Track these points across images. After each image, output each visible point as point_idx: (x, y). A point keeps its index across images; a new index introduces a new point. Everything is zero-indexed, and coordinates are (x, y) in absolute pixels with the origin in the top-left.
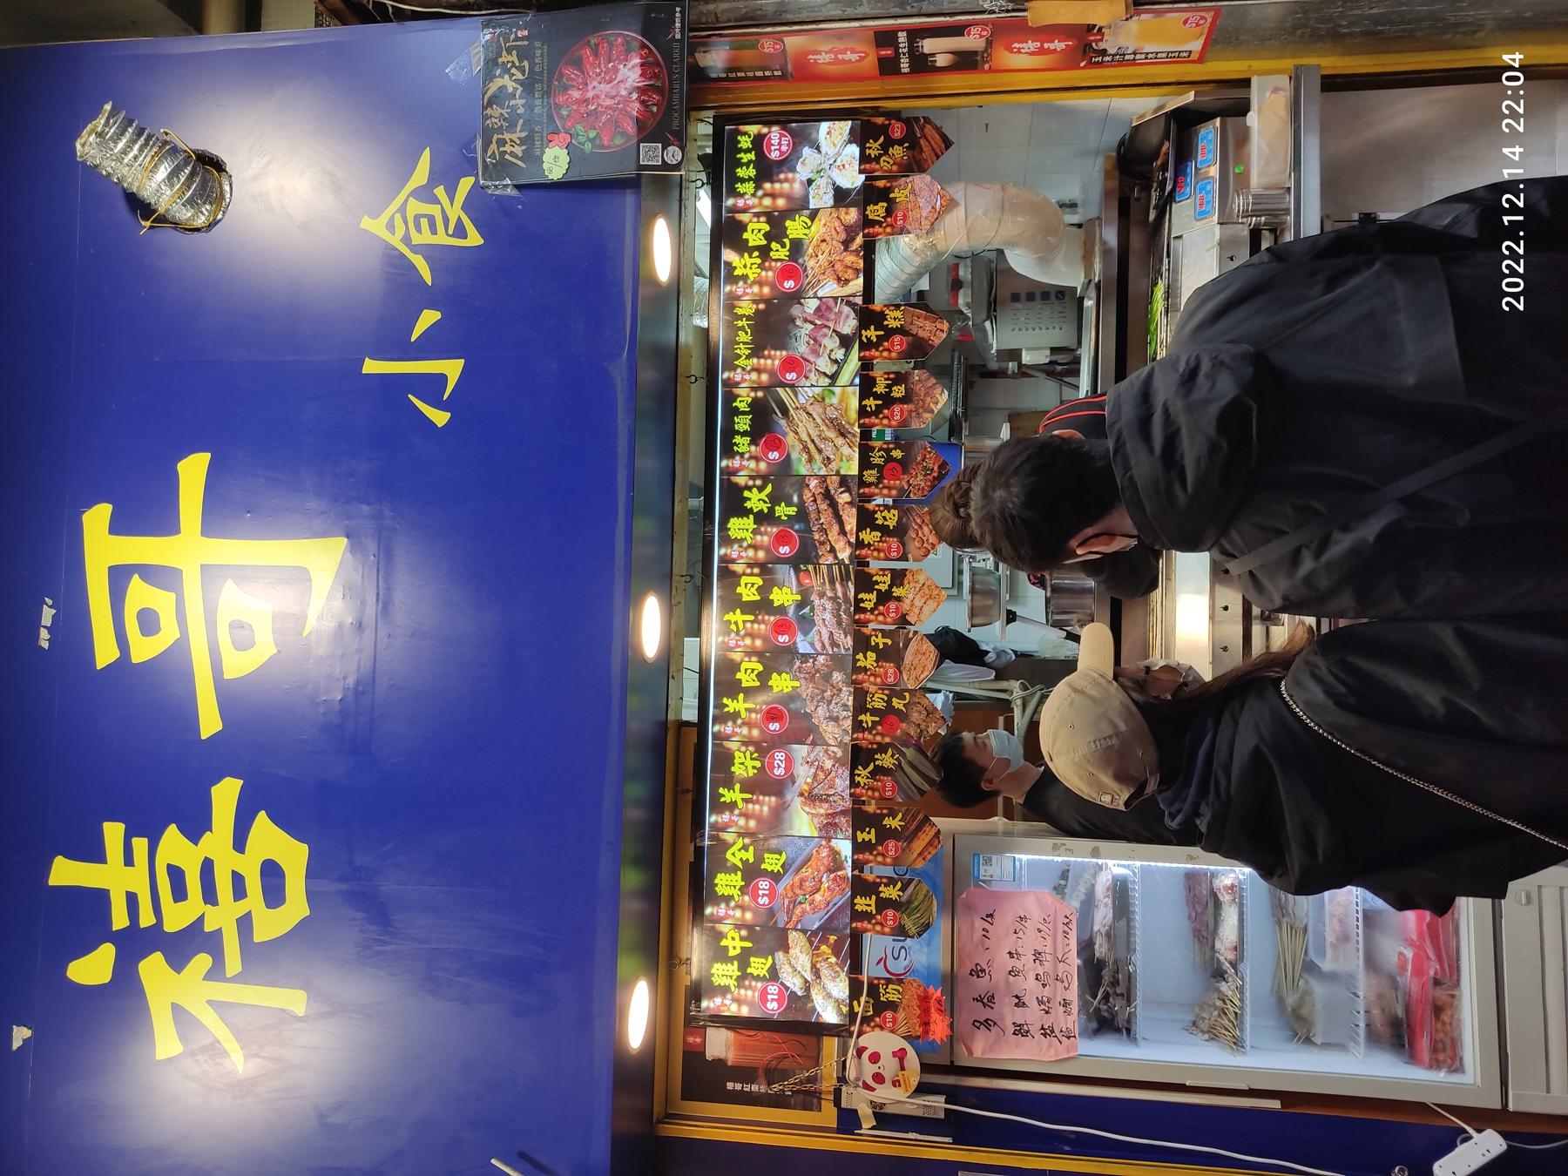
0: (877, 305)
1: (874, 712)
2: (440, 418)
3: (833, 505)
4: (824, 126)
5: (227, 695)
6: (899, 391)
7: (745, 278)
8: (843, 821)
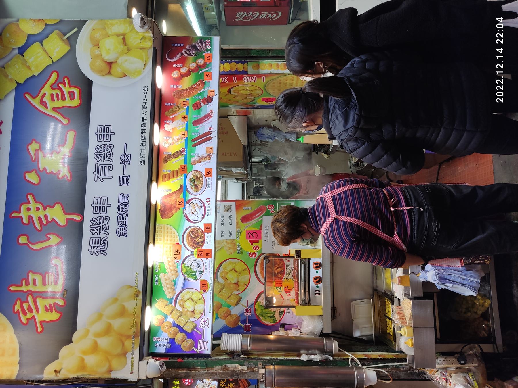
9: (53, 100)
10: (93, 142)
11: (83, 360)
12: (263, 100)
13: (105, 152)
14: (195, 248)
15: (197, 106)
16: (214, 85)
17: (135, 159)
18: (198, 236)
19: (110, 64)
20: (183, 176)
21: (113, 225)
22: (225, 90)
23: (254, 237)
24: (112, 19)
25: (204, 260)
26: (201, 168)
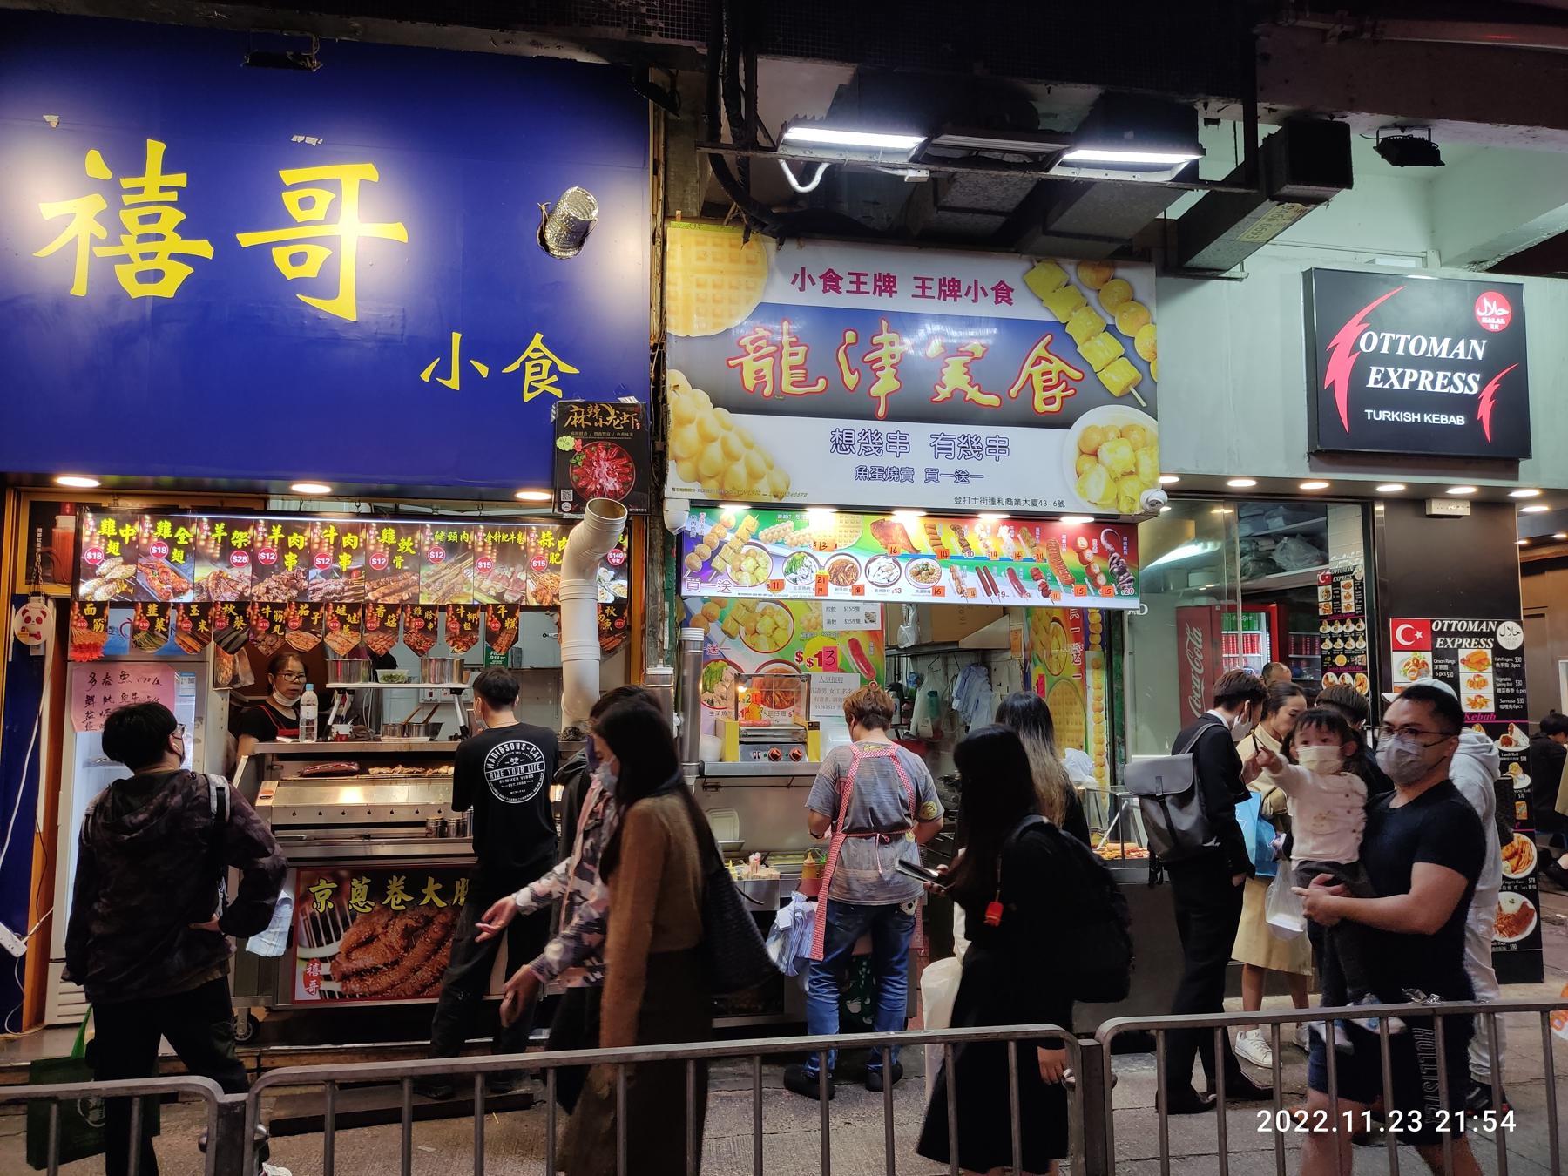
0: (518, 614)
1: (272, 615)
2: (426, 376)
3: (401, 590)
4: (625, 583)
5: (264, 250)
6: (467, 626)
7: (540, 538)
8: (204, 597)
9: (1044, 374)
10: (984, 432)
11: (690, 421)
12: (1041, 677)
13: (971, 448)
14: (830, 571)
15: (1036, 574)
16: (1069, 600)
17: (962, 490)
18: (847, 575)
19: (1095, 454)
20: (932, 553)
21: (871, 461)
22: (1057, 614)
23: (827, 659)
24: (1160, 456)
25: (813, 585)
26: (946, 580)
